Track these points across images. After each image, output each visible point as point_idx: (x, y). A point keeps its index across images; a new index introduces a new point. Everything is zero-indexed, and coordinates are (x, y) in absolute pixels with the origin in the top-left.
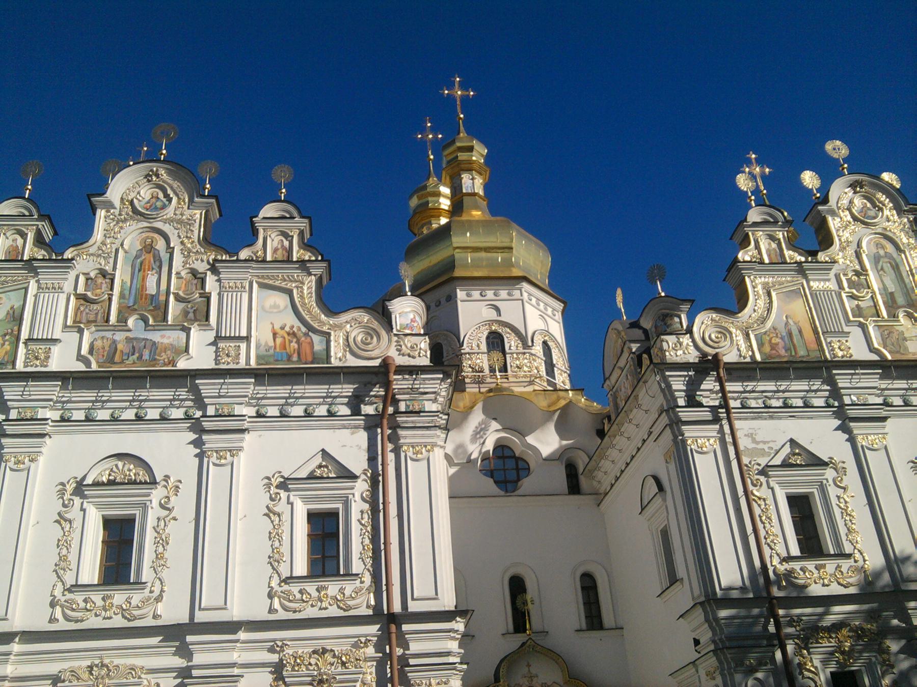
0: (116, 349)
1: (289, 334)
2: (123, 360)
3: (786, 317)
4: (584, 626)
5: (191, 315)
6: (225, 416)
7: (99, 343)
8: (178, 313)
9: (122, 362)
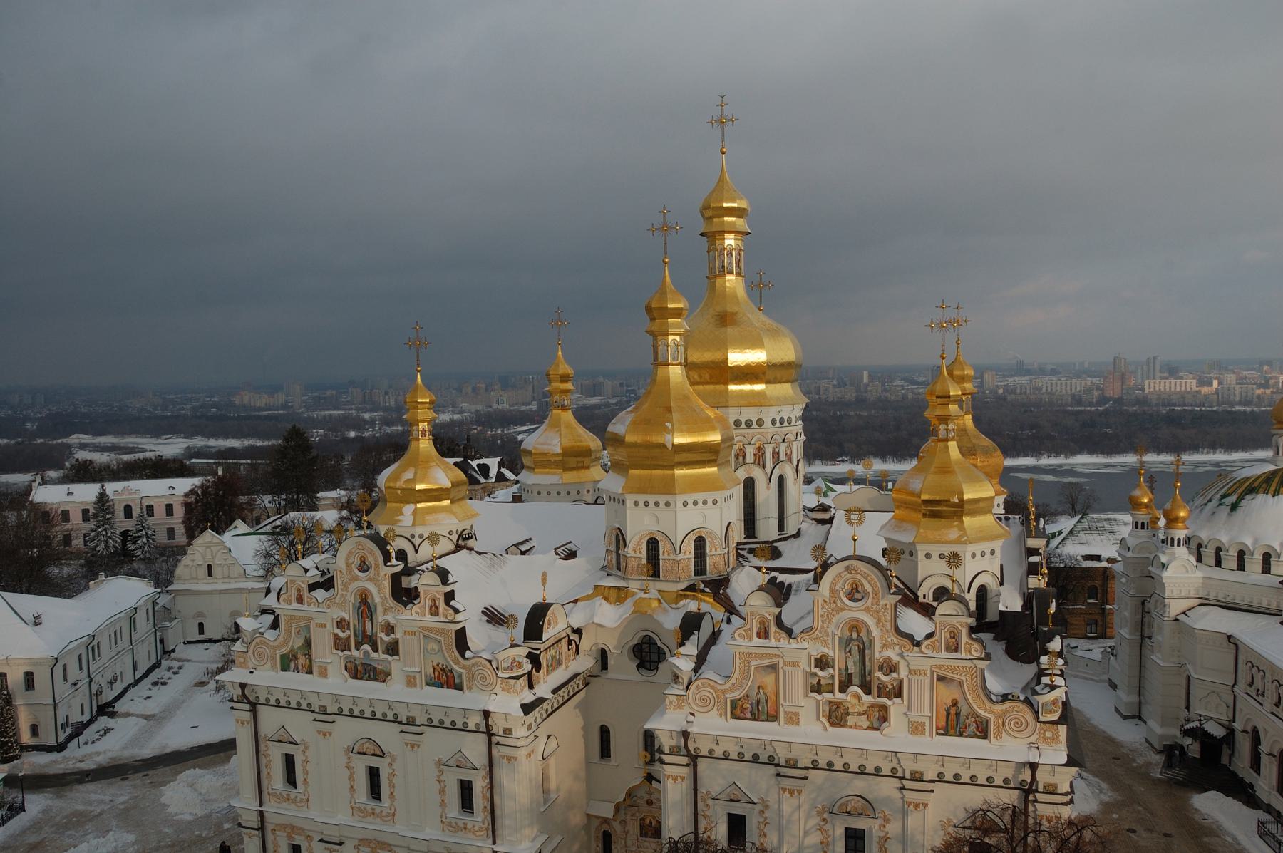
1: (441, 669)
3: (759, 688)
5: (390, 651)
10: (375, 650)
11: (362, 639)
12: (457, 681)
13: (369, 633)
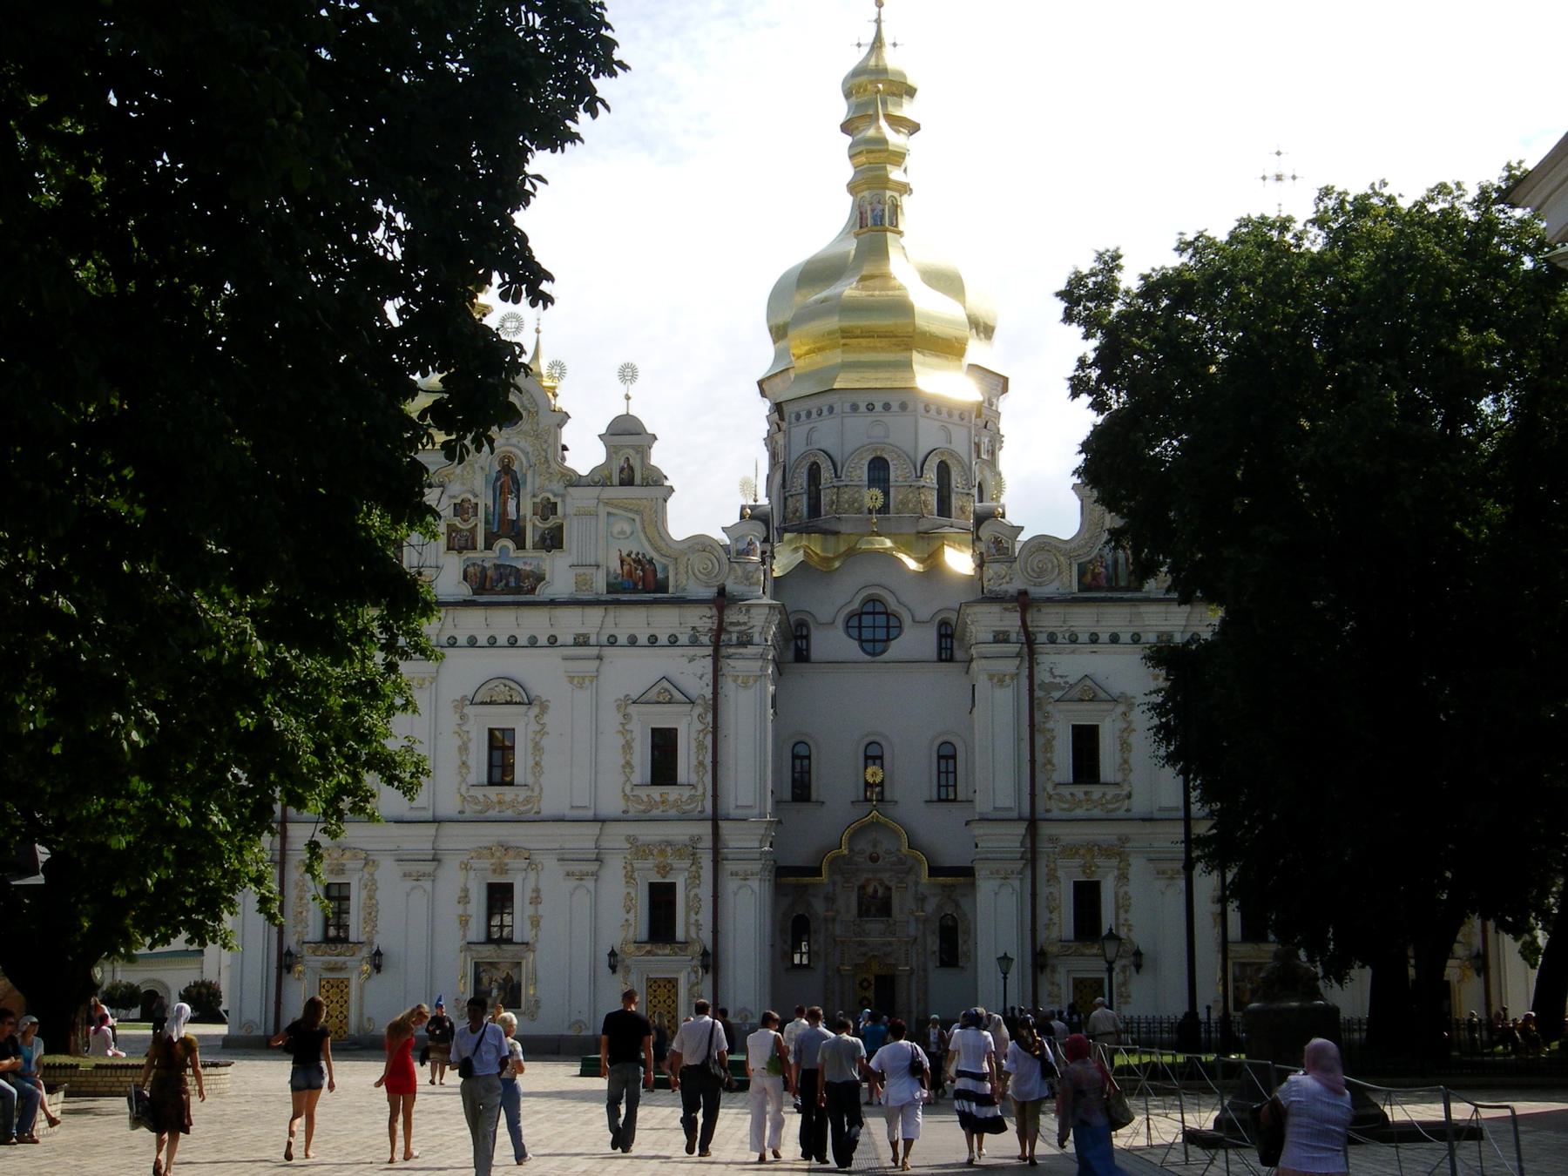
0: (486, 575)
1: (634, 561)
2: (493, 587)
4: (935, 797)
5: (548, 541)
6: (581, 646)
7: (471, 570)
8: (537, 539)
9: (492, 589)
10: (521, 545)
11: (499, 528)
12: (660, 575)
13: (512, 515)
